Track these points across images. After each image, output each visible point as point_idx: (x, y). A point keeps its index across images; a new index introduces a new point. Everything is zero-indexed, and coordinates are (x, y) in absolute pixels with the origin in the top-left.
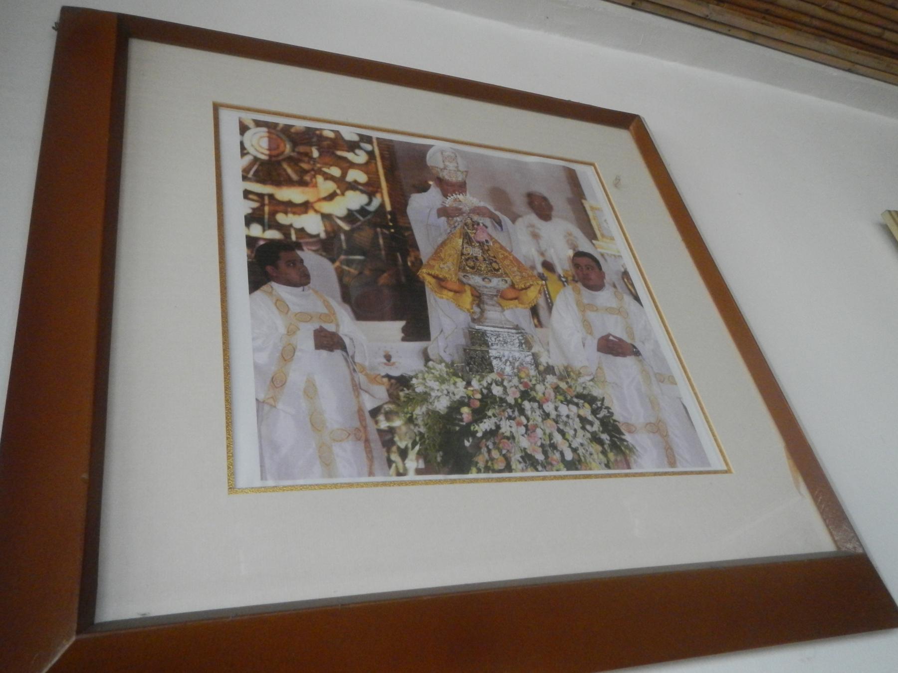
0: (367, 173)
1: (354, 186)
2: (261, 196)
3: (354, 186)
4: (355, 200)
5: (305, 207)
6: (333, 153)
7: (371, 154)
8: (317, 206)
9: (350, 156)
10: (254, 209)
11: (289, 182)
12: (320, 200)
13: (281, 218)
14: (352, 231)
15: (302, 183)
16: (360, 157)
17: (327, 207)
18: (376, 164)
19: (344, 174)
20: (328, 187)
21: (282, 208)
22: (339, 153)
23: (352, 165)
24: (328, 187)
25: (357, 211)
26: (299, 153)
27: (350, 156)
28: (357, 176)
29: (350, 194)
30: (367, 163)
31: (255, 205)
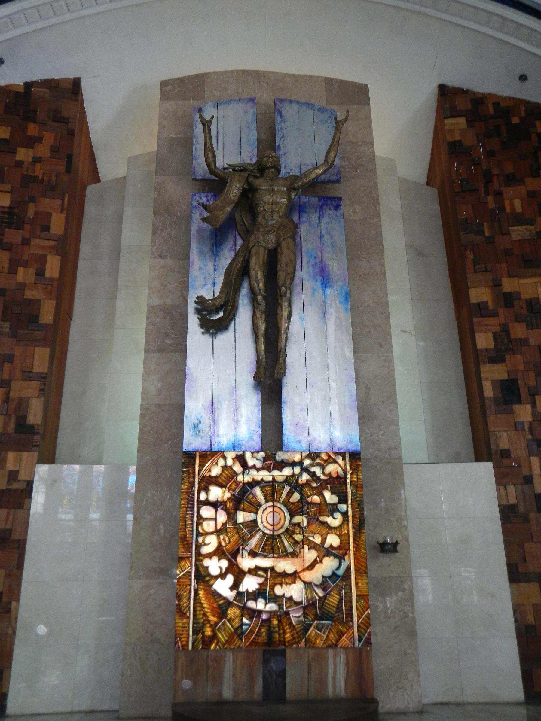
0: (340, 536)
1: (329, 552)
2: (265, 570)
3: (329, 552)
4: (329, 565)
5: (295, 576)
6: (318, 519)
7: (345, 514)
8: (301, 575)
9: (329, 520)
10: (260, 584)
11: (286, 555)
12: (304, 570)
13: (278, 591)
14: (325, 597)
15: (294, 555)
16: (335, 521)
17: (309, 576)
18: (348, 525)
19: (324, 540)
20: (310, 555)
21: (279, 580)
22: (321, 518)
23: (330, 528)
24: (310, 555)
25: (330, 577)
26: (295, 525)
27: (329, 520)
28: (333, 540)
29: (326, 560)
30: (340, 527)
31: (261, 580)
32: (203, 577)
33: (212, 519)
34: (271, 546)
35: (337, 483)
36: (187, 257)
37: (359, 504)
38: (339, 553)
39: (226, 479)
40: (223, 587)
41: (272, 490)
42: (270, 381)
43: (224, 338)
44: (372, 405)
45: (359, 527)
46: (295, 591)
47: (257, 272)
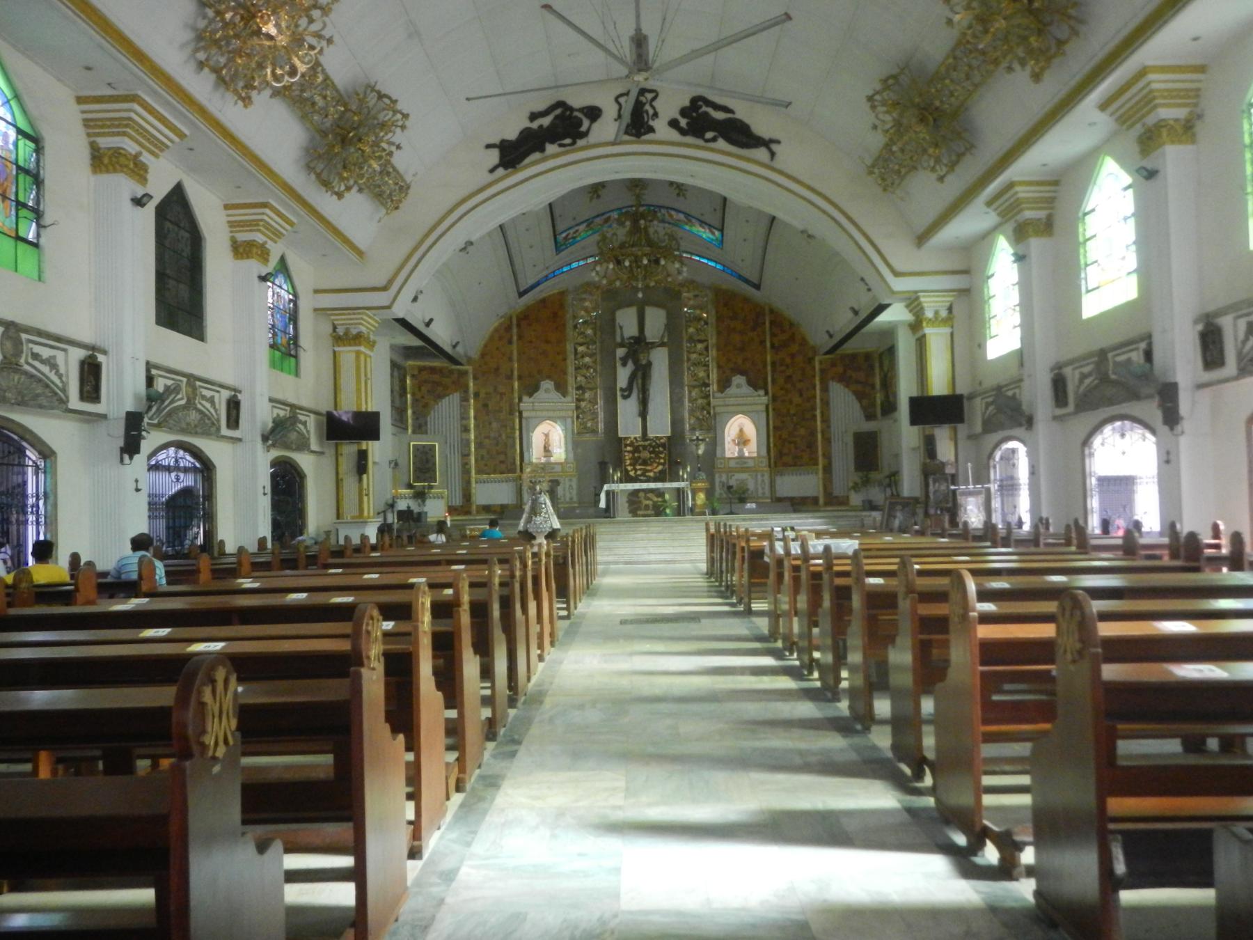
3: (659, 464)
4: (660, 468)
32: (627, 472)
33: (628, 456)
34: (645, 463)
35: (663, 445)
36: (615, 368)
37: (670, 453)
38: (663, 464)
39: (631, 444)
40: (632, 473)
41: (645, 447)
42: (643, 414)
43: (629, 400)
44: (676, 423)
45: (670, 456)
46: (651, 474)
47: (640, 374)
